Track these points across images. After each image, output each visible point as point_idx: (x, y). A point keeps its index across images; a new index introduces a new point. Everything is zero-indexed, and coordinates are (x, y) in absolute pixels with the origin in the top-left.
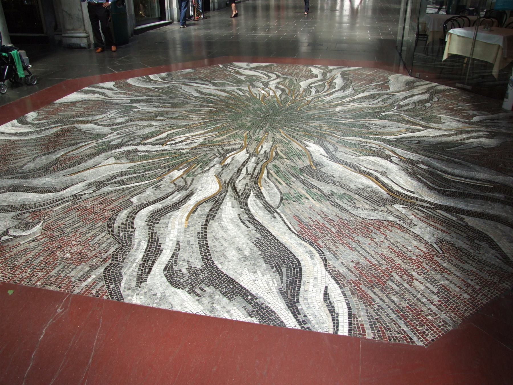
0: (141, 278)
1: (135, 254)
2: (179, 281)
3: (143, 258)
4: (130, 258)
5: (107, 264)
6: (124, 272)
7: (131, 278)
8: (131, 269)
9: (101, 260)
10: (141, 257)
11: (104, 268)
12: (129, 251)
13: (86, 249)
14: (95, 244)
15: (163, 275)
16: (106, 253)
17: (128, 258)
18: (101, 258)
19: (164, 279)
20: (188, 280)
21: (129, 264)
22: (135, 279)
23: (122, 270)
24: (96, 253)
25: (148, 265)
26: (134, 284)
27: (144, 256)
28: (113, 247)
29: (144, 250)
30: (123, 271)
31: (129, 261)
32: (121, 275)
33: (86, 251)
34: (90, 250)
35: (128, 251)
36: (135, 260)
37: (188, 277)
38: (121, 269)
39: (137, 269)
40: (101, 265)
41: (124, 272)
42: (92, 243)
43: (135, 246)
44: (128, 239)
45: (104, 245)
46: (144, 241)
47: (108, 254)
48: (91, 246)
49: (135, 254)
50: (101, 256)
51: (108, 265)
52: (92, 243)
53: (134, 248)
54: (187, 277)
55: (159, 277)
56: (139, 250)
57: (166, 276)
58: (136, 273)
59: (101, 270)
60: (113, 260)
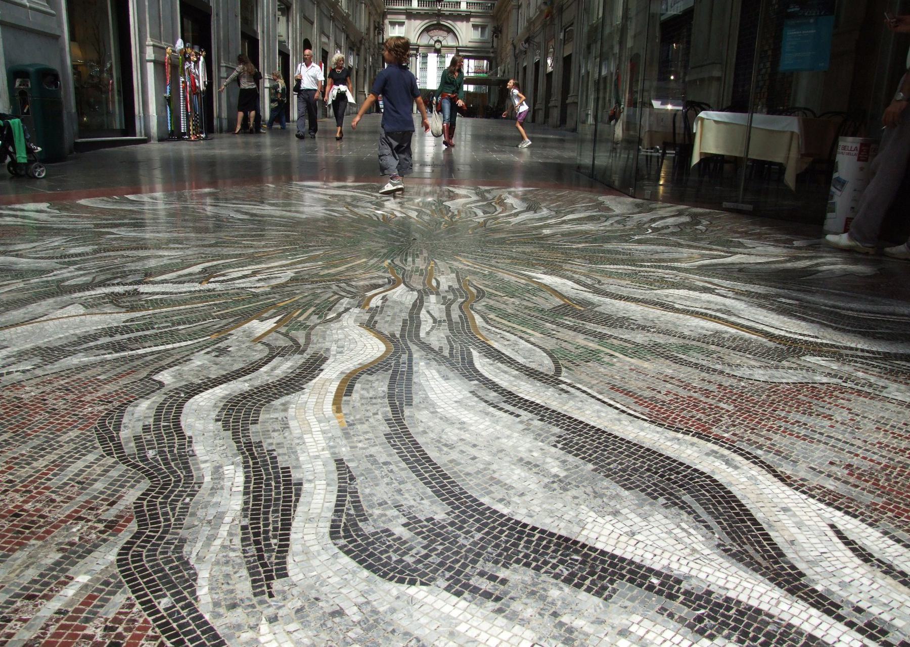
0: (264, 565)
1: (214, 500)
2: (401, 561)
3: (244, 510)
4: (201, 513)
5: (125, 536)
6: (194, 554)
7: (228, 569)
8: (218, 542)
9: (101, 526)
10: (239, 508)
11: (116, 550)
12: (193, 495)
13: (37, 501)
14: (66, 484)
15: (337, 550)
16: (112, 504)
17: (193, 514)
18: (100, 521)
19: (346, 560)
20: (427, 556)
21: (206, 530)
22: (244, 572)
23: (186, 549)
24: (75, 508)
25: (271, 527)
26: (243, 587)
27: (246, 503)
28: (133, 486)
29: (241, 489)
30: (191, 552)
31: (201, 521)
32: (187, 563)
33: (39, 505)
34: (53, 501)
35: (188, 495)
36: (220, 517)
37: (424, 548)
38: (179, 548)
39: (237, 541)
40: (105, 540)
41: (194, 554)
42: (56, 482)
43: (207, 479)
44: (176, 465)
45: (99, 486)
46: (232, 467)
47: (122, 508)
48: (53, 492)
49: (214, 500)
50: (97, 515)
51: (128, 538)
52: (56, 482)
53: (204, 486)
54: (419, 548)
55: (324, 557)
56: (222, 488)
57: (348, 553)
58: (239, 554)
59: (107, 556)
60: (142, 523)
